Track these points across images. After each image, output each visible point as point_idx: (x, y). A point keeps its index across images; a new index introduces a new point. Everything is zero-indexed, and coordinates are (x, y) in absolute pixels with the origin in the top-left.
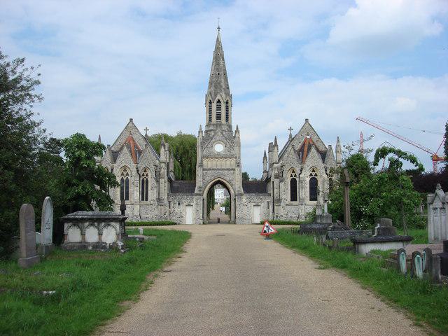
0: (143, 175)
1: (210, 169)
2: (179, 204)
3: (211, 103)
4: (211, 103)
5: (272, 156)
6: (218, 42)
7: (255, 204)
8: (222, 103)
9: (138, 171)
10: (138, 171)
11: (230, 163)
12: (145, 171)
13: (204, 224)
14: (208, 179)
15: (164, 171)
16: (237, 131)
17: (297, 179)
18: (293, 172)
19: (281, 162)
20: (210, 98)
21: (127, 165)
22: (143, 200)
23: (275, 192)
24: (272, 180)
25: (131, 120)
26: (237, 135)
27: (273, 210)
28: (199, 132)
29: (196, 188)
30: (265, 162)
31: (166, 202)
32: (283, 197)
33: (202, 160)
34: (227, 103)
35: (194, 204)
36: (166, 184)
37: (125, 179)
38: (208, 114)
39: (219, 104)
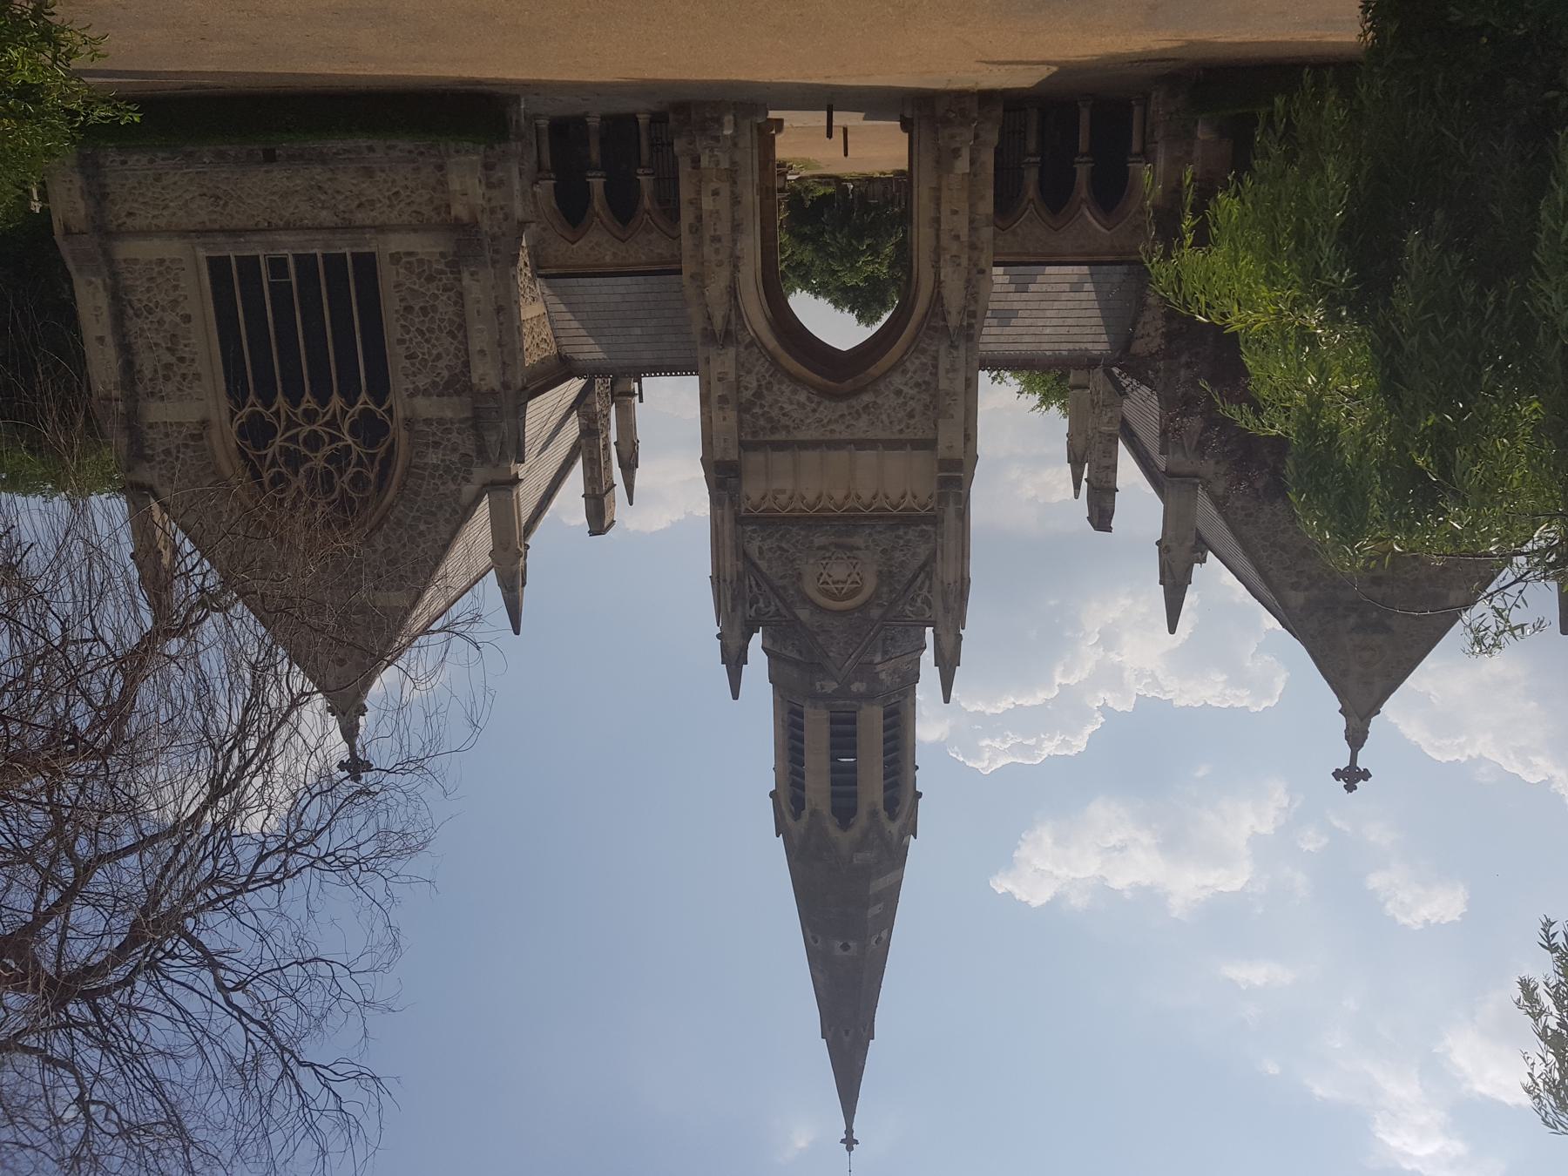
8: (825, 808)
16: (734, 660)
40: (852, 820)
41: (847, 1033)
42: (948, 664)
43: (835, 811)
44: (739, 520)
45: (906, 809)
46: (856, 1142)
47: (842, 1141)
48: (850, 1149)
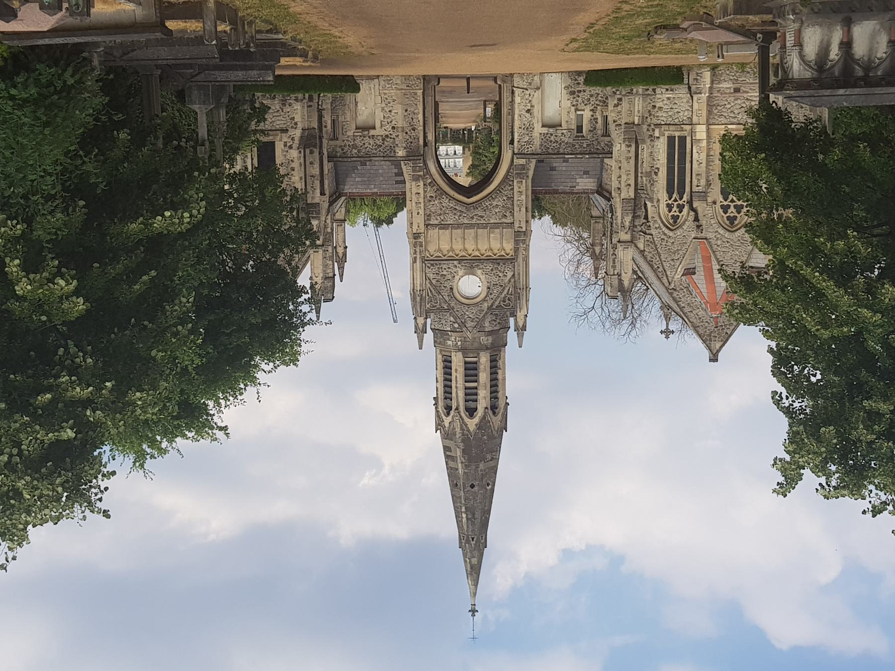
1: (496, 226)
5: (325, 266)
6: (474, 571)
7: (372, 132)
8: (462, 409)
13: (512, 75)
15: (622, 217)
23: (317, 165)
24: (326, 198)
27: (320, 117)
31: (617, 136)
35: (538, 129)
39: (471, 405)
40: (475, 413)
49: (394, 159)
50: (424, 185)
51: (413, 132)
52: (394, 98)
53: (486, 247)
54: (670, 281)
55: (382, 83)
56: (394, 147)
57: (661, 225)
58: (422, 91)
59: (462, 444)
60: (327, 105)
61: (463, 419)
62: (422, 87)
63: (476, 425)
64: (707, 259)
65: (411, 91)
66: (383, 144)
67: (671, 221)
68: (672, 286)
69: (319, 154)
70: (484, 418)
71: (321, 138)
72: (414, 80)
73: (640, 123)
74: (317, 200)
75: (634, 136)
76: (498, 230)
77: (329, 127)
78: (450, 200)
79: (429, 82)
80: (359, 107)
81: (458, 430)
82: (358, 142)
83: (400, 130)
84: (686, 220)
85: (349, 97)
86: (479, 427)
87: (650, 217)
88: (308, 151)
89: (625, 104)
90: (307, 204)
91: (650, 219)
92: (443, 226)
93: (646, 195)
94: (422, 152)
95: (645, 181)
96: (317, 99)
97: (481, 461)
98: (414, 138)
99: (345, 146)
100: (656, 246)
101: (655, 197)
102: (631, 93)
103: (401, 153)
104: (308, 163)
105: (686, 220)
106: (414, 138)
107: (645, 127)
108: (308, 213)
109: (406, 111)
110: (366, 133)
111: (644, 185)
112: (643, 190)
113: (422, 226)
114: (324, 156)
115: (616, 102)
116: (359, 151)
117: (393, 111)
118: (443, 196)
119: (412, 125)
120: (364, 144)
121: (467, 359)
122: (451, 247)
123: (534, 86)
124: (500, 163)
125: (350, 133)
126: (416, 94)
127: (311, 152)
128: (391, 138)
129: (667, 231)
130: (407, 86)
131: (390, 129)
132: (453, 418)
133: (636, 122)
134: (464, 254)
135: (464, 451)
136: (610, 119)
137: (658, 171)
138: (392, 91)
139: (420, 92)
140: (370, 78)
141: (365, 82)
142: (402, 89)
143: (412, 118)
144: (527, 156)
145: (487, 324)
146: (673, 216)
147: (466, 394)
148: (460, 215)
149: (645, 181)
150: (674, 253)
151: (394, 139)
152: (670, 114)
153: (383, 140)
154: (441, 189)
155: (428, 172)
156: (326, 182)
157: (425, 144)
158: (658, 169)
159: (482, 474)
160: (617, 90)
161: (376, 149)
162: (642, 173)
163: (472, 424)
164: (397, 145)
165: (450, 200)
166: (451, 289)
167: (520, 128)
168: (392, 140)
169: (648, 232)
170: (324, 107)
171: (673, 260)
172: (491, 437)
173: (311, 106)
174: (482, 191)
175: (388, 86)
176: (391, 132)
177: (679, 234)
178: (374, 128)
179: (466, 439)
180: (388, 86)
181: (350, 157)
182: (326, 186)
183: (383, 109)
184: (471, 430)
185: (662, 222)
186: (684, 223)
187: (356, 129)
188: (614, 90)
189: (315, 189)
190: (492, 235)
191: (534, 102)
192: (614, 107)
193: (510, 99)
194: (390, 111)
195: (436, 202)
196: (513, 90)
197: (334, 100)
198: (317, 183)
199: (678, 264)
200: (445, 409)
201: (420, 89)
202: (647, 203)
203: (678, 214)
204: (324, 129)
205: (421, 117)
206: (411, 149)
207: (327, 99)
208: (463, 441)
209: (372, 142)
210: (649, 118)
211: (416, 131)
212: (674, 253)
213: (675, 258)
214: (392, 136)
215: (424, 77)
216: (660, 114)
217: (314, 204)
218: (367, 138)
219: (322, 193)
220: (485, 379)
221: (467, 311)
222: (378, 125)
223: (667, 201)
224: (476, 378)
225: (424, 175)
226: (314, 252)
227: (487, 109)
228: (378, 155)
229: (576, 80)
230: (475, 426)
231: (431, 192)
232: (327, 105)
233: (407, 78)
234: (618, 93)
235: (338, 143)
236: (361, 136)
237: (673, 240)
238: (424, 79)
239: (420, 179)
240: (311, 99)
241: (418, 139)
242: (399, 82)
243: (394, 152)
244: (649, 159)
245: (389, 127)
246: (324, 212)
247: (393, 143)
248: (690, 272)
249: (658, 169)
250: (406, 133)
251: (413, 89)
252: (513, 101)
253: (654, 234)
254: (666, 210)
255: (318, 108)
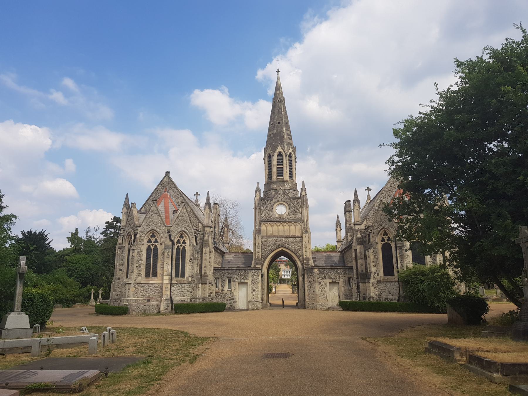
0: (178, 242)
1: (269, 237)
2: (230, 282)
3: (270, 157)
4: (270, 157)
7: (331, 281)
8: (284, 155)
9: (170, 236)
10: (170, 236)
11: (295, 230)
12: (181, 237)
13: (263, 308)
14: (268, 248)
16: (303, 189)
17: (393, 245)
18: (386, 234)
19: (365, 223)
20: (269, 151)
21: (155, 228)
22: (177, 275)
23: (359, 264)
24: (353, 248)
25: (167, 173)
26: (303, 194)
28: (256, 191)
29: (253, 261)
30: (339, 228)
32: (373, 270)
33: (260, 226)
34: (290, 156)
36: (213, 254)
37: (152, 247)
38: (267, 170)
39: (280, 158)
41: (279, 101)
42: (258, 190)
43: (282, 156)
44: (302, 221)
45: (266, 155)
46: (277, 72)
47: (280, 72)
48: (278, 70)
49: (319, 268)
50: (303, 256)
51: (310, 281)
52: (320, 298)
53: (274, 228)
54: (184, 207)
55: (326, 305)
56: (319, 273)
57: (188, 234)
58: (306, 301)
59: (284, 140)
60: (355, 295)
61: (284, 151)
62: (306, 304)
63: (278, 149)
64: (167, 217)
65: (311, 301)
66: (325, 275)
67: (183, 235)
68: (183, 204)
69: (358, 270)
70: (274, 152)
71: (357, 278)
72: (310, 307)
73: (198, 284)
74: (359, 247)
75: (202, 278)
76: (268, 235)
77: (353, 284)
78: (291, 249)
79: (302, 305)
80: (337, 294)
81: (286, 146)
82: (338, 276)
83: (317, 282)
84: (176, 236)
85: (343, 299)
86: (276, 148)
87: (194, 238)
88: (364, 271)
89: (207, 294)
90: (363, 245)
91: (194, 237)
92: (294, 237)
93: (195, 248)
94: (305, 271)
95: (196, 255)
96: (361, 298)
97: (275, 133)
98: (309, 278)
99: (344, 274)
100: (191, 224)
101: (192, 248)
102: (203, 300)
103: (316, 270)
104: (364, 265)
105: (176, 236)
106: (309, 278)
107: (196, 282)
108: (363, 240)
109: (314, 291)
110: (334, 280)
111: (196, 253)
112: (197, 251)
113: (304, 237)
114: (356, 269)
115: (211, 295)
116: (337, 271)
117: (320, 291)
118: (294, 250)
119: (310, 284)
120: (334, 275)
121: (282, 177)
122: (290, 227)
123: (252, 303)
124: (268, 266)
125: (342, 280)
126: (309, 300)
127: (362, 271)
128: (321, 278)
129: (186, 231)
130: (313, 303)
131: (322, 282)
132: (288, 151)
133: (200, 284)
134: (284, 224)
135: (283, 137)
136: (214, 286)
137: (190, 260)
138: (321, 301)
139: (307, 300)
140: (332, 308)
141: (335, 306)
142: (316, 302)
143: (311, 287)
144: (254, 268)
145: (273, 193)
146: (183, 238)
147: (282, 162)
148: (286, 242)
149: (196, 255)
150: (182, 220)
151: (320, 278)
152: (183, 289)
153: (325, 277)
154: (295, 254)
155: (301, 262)
156: (354, 256)
157: (304, 275)
158: (190, 262)
159: (275, 128)
160: (211, 300)
161: (328, 272)
162: (198, 259)
163: (279, 149)
164: (318, 274)
165: (291, 249)
166: (289, 208)
167: (258, 282)
168: (320, 277)
169: (196, 231)
170: (356, 294)
171: (183, 217)
172: (271, 144)
173: (364, 294)
174: (276, 253)
175: (323, 304)
176: (321, 281)
177: (179, 229)
178: (330, 283)
179: (282, 143)
180: (323, 304)
181: (341, 268)
182: (354, 254)
183: (326, 292)
184: (280, 146)
185: (188, 235)
186: (177, 234)
187: (338, 283)
188: (212, 301)
189: (360, 252)
190: (271, 233)
191: (251, 295)
192: (212, 292)
193: (263, 296)
194: (322, 291)
195: (297, 248)
196: (262, 300)
197: (351, 297)
198: (359, 255)
199: (180, 215)
200: (291, 156)
201: (307, 302)
202: (196, 245)
203: (180, 239)
204: (356, 282)
205: (306, 288)
206: (311, 272)
207: (355, 298)
208: (283, 142)
209: (331, 276)
210: (194, 286)
211: (309, 281)
212: (182, 220)
213: (182, 217)
214: (321, 279)
215: (304, 307)
216: (188, 289)
217: (360, 245)
218: (333, 278)
219: (356, 250)
220: (274, 169)
221: (282, 198)
222: (328, 284)
223: (186, 246)
224: (278, 169)
225: (303, 260)
226: (358, 221)
227: (274, 290)
228: (327, 269)
229: (231, 306)
230: (278, 148)
231: (300, 252)
232: (355, 295)
233: (314, 308)
234: (210, 299)
235: (347, 276)
236: (336, 279)
237: (183, 226)
238: (305, 306)
239: (305, 259)
240: (364, 298)
241: (307, 278)
242: (318, 306)
243: (319, 271)
244: (194, 266)
245: (322, 283)
246: (354, 241)
247: (320, 276)
248: (175, 212)
249: (190, 261)
250: (313, 280)
251: (311, 302)
252: (262, 295)
253: (192, 230)
254: (186, 241)
255: (360, 293)
